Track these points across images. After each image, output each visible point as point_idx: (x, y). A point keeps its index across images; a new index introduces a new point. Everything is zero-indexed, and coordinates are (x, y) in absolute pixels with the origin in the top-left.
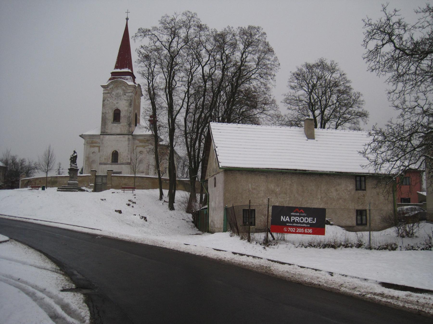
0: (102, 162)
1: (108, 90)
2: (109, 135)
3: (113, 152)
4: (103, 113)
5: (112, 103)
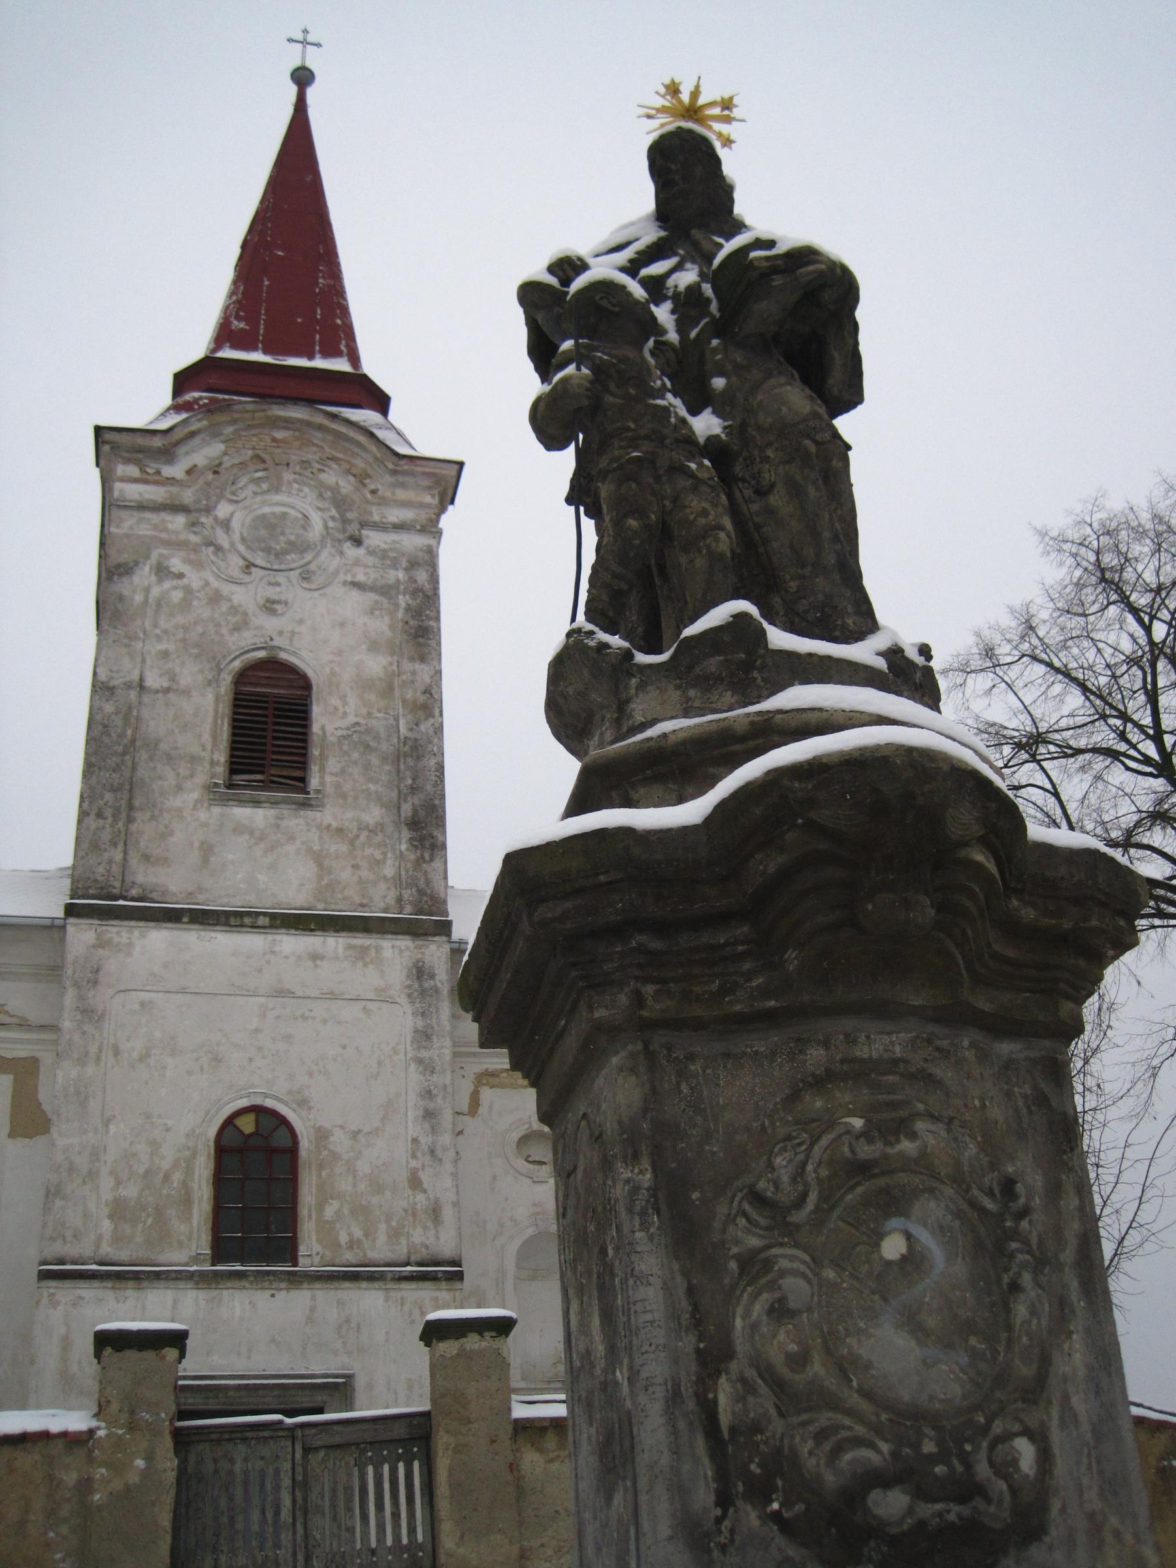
0: (84, 1248)
1: (172, 481)
2: (172, 917)
3: (229, 1122)
4: (101, 689)
5: (216, 598)
